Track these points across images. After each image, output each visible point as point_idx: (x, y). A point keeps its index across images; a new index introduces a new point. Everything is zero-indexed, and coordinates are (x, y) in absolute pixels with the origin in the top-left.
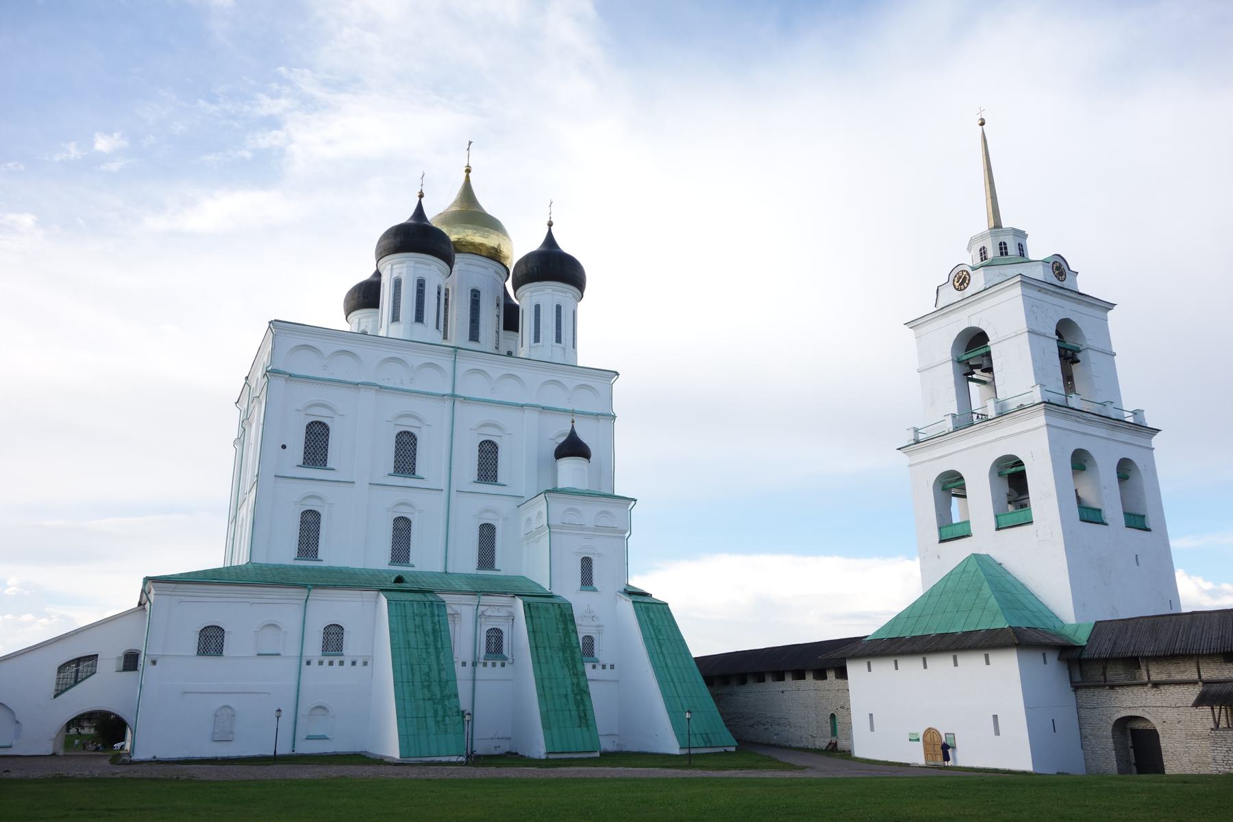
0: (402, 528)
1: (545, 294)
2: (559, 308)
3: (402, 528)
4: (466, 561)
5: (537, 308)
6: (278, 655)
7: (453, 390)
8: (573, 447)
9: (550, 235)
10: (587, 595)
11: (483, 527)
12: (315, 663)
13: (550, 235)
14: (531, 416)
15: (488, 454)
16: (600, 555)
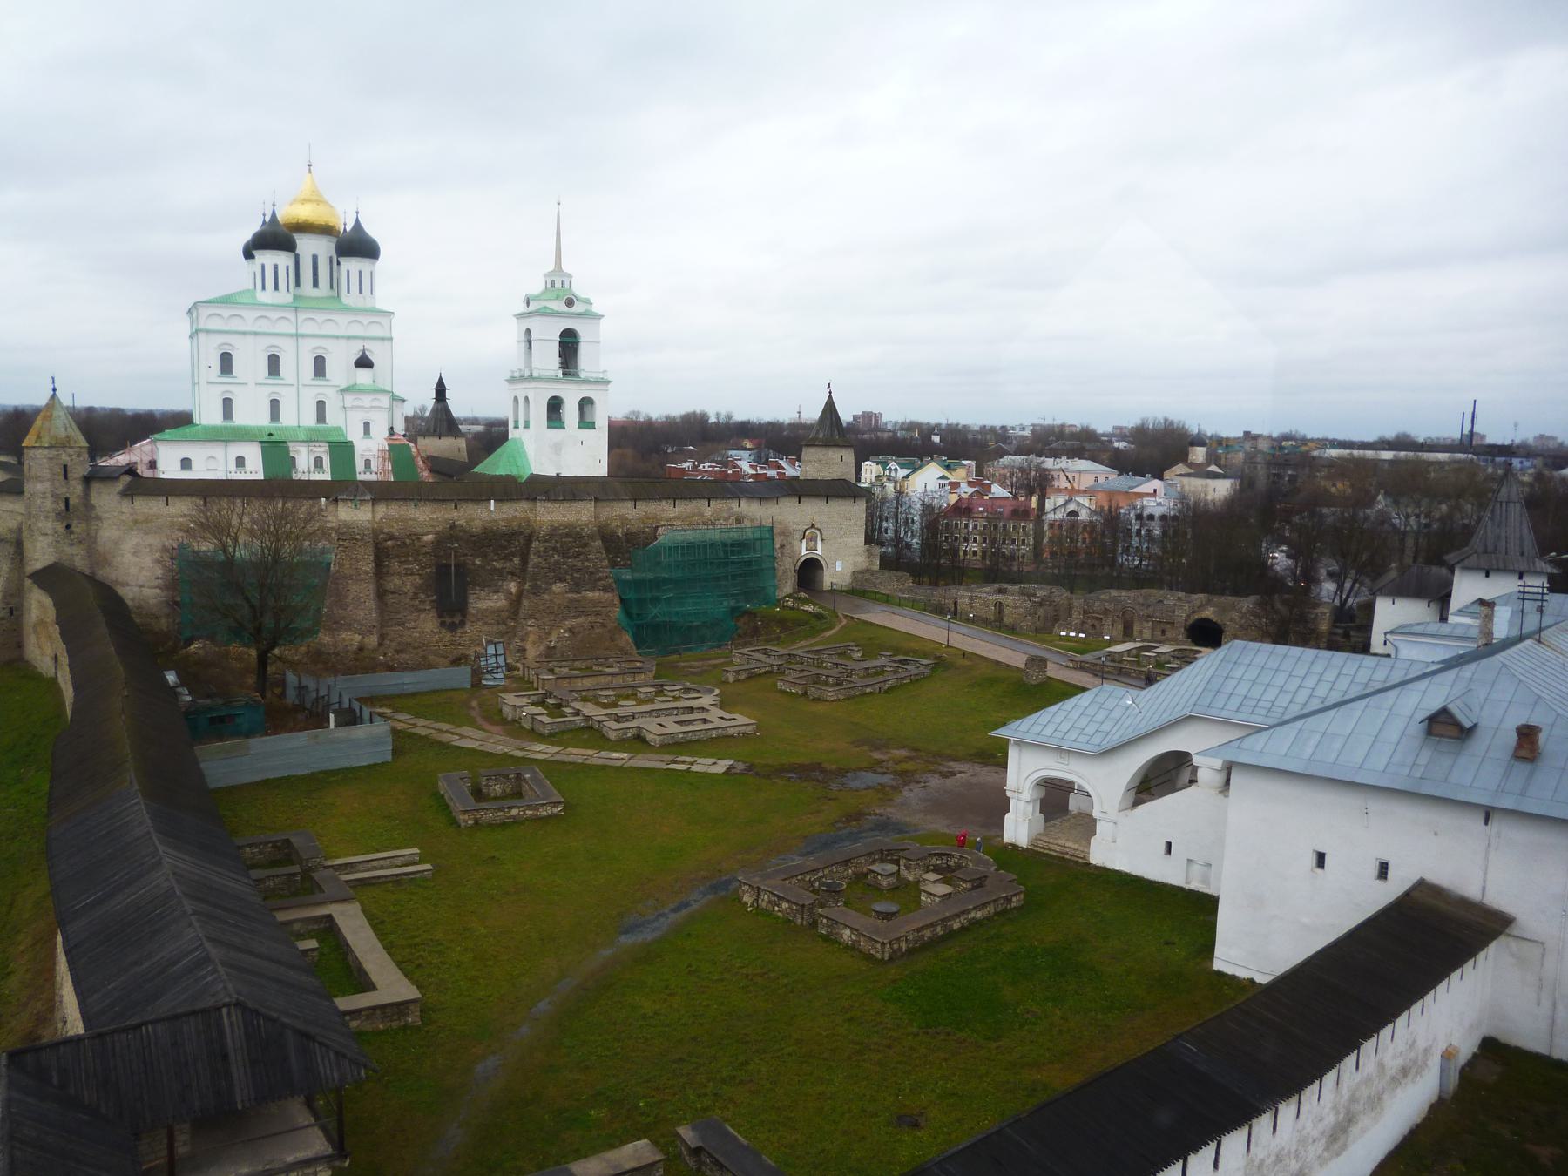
0: (275, 404)
1: (351, 265)
2: (360, 272)
3: (275, 404)
4: (310, 420)
5: (348, 272)
6: (216, 470)
7: (297, 329)
8: (364, 362)
9: (357, 219)
10: (367, 441)
11: (318, 402)
12: (233, 472)
13: (357, 219)
14: (343, 342)
15: (320, 366)
16: (373, 421)
